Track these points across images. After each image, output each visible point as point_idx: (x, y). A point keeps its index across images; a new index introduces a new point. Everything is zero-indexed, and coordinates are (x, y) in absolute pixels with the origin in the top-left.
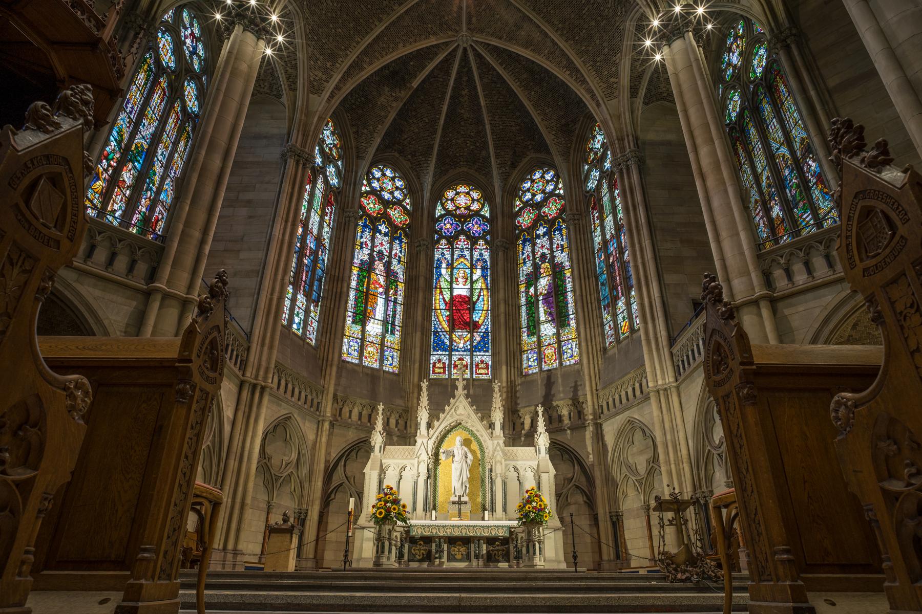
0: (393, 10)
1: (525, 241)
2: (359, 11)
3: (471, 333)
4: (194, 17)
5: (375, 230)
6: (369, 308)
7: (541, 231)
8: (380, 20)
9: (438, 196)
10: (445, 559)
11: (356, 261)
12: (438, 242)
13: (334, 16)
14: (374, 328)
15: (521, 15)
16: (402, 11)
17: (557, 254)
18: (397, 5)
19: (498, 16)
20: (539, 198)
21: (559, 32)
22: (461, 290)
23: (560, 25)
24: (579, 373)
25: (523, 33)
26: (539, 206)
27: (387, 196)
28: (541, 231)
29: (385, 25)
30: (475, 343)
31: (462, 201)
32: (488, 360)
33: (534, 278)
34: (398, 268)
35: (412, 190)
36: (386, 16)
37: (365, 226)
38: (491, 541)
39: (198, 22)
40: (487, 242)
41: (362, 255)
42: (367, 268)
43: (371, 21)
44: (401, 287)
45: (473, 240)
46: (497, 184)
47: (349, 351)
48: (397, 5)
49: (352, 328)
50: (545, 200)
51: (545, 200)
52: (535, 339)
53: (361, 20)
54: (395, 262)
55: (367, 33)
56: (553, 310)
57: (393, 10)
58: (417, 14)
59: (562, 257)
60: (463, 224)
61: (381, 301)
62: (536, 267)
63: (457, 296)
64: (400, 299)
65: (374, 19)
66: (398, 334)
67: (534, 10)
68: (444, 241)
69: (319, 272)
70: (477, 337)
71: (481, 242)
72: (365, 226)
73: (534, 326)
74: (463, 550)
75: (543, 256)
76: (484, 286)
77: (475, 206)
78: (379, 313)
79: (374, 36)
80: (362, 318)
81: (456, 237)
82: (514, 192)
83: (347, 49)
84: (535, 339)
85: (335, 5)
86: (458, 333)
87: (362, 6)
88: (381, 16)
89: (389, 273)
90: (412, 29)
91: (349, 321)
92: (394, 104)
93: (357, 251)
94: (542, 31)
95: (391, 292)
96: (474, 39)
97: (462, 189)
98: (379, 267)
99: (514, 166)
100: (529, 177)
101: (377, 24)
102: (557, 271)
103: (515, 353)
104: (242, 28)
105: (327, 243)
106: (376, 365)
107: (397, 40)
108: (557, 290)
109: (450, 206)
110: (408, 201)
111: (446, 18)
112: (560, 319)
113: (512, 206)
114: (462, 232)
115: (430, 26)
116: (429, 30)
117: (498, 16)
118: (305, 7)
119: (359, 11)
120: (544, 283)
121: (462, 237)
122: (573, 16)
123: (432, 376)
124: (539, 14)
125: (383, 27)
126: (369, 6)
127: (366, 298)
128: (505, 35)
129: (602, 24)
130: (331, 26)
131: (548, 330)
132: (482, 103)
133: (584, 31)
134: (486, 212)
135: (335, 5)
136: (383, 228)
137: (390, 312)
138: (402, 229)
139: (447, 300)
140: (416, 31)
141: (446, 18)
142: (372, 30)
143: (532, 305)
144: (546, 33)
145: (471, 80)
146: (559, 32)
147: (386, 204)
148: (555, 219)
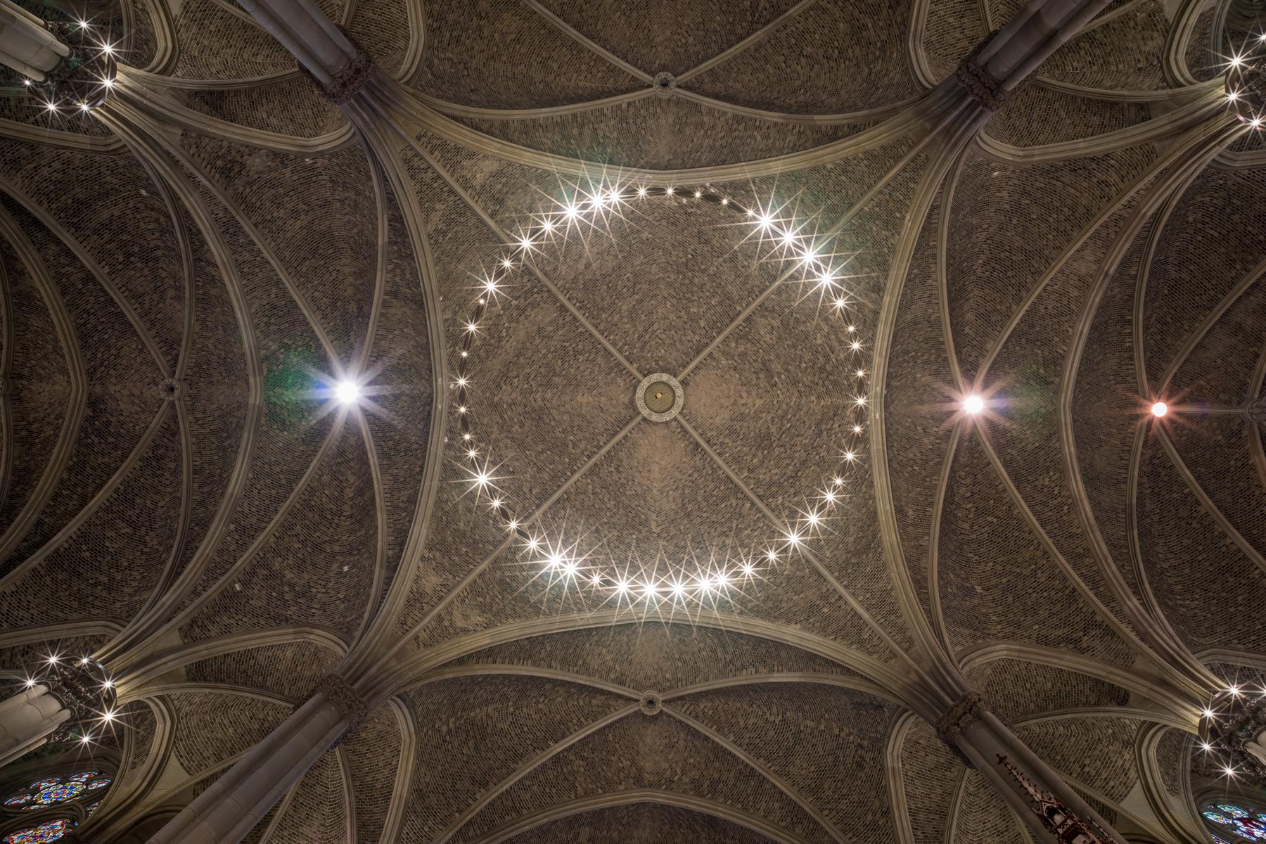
0: (1207, 514)
2: (1207, 564)
4: (1215, 806)
8: (1224, 535)
13: (1215, 601)
15: (1218, 327)
16: (1210, 502)
18: (1199, 508)
19: (1219, 361)
21: (1251, 266)
23: (1238, 267)
25: (1249, 322)
29: (1233, 529)
36: (1216, 526)
39: (1224, 804)
43: (1224, 549)
48: (1199, 508)
53: (1223, 564)
55: (1245, 557)
57: (1207, 514)
58: (1213, 480)
65: (1221, 544)
67: (1210, 309)
79: (1251, 548)
85: (1197, 596)
87: (1200, 558)
88: (1216, 534)
90: (1238, 489)
94: (1247, 293)
96: (1256, 396)
101: (1229, 541)
104: (1251, 744)
107: (1258, 513)
111: (1220, 437)
115: (1232, 463)
116: (1239, 464)
117: (1219, 361)
118: (1202, 641)
119: (1207, 564)
122: (1223, 250)
124: (1217, 301)
125: (1236, 532)
126: (1200, 548)
128: (1251, 349)
129: (1239, 203)
130: (1232, 610)
133: (1250, 228)
135: (1197, 596)
140: (1241, 484)
141: (1220, 437)
142: (1239, 550)
144: (1252, 287)
146: (1251, 266)
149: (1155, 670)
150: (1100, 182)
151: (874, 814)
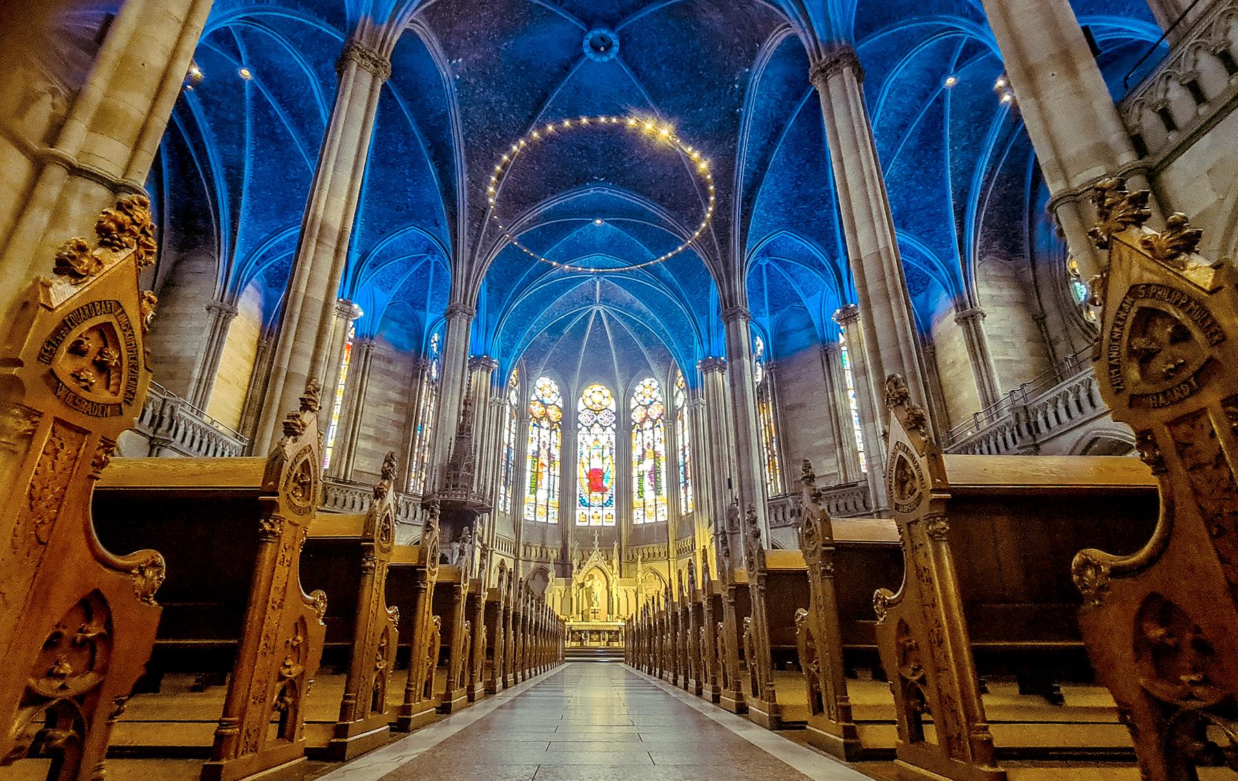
1: (638, 430)
3: (602, 494)
5: (540, 427)
6: (539, 483)
7: (648, 424)
9: (579, 395)
10: (588, 641)
11: (530, 452)
12: (580, 429)
14: (542, 495)
17: (657, 444)
20: (647, 401)
22: (597, 464)
24: (667, 526)
26: (647, 407)
27: (547, 401)
28: (648, 424)
30: (605, 502)
31: (597, 398)
32: (613, 513)
33: (642, 459)
34: (556, 452)
35: (565, 394)
37: (534, 425)
38: (610, 632)
40: (613, 430)
41: (531, 447)
42: (537, 455)
44: (558, 465)
45: (604, 428)
46: (621, 389)
47: (528, 515)
49: (528, 497)
50: (651, 403)
51: (651, 403)
52: (642, 500)
54: (553, 447)
56: (653, 483)
59: (660, 448)
60: (597, 415)
61: (546, 475)
62: (644, 451)
63: (594, 469)
64: (557, 473)
66: (557, 497)
68: (584, 429)
69: (510, 466)
70: (606, 498)
71: (609, 429)
72: (534, 425)
73: (641, 492)
74: (597, 636)
75: (649, 444)
76: (611, 462)
77: (605, 402)
78: (545, 486)
80: (535, 489)
81: (592, 426)
82: (629, 394)
83: (523, 325)
84: (642, 500)
86: (594, 494)
89: (550, 456)
91: (527, 493)
92: (551, 344)
93: (529, 444)
95: (552, 469)
97: (597, 388)
98: (544, 453)
99: (632, 376)
100: (641, 382)
102: (656, 456)
103: (630, 507)
105: (512, 445)
106: (545, 520)
108: (655, 472)
109: (589, 402)
110: (560, 400)
112: (657, 490)
113: (629, 404)
114: (597, 422)
120: (648, 464)
121: (596, 425)
123: (578, 524)
127: (537, 474)
131: (649, 495)
132: (610, 339)
134: (613, 407)
136: (545, 424)
137: (552, 483)
138: (557, 422)
139: (588, 472)
143: (641, 477)
145: (602, 323)
147: (545, 406)
148: (658, 418)
149: (490, 324)
150: (699, 290)
151: (379, 226)
